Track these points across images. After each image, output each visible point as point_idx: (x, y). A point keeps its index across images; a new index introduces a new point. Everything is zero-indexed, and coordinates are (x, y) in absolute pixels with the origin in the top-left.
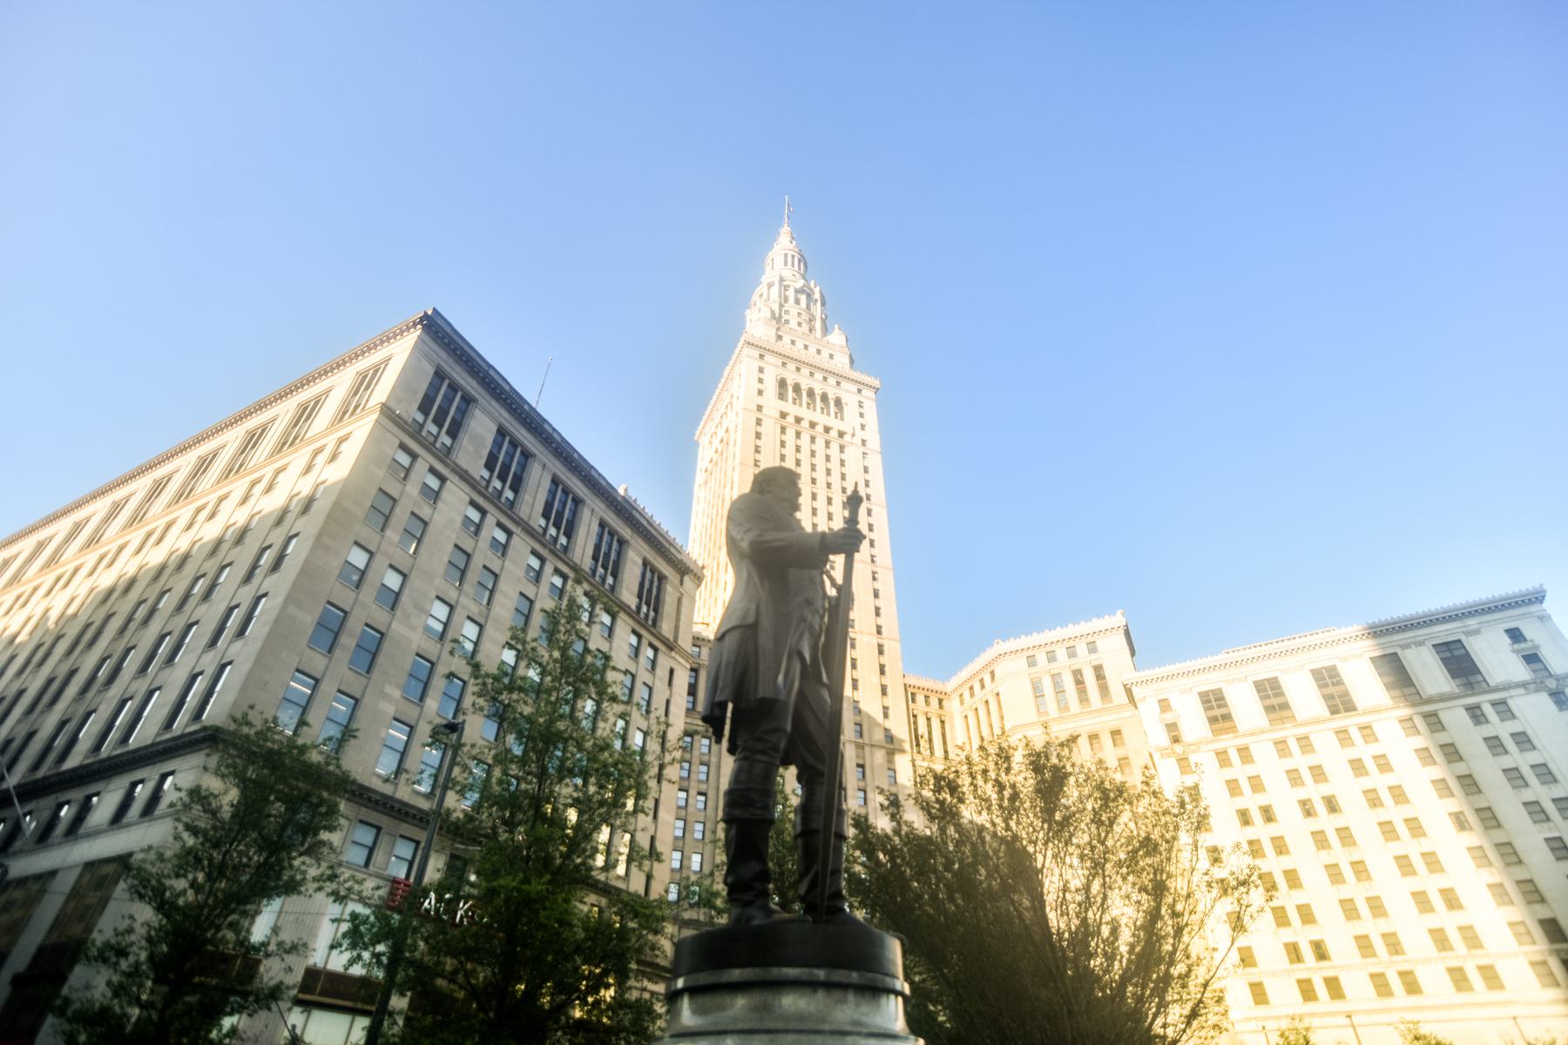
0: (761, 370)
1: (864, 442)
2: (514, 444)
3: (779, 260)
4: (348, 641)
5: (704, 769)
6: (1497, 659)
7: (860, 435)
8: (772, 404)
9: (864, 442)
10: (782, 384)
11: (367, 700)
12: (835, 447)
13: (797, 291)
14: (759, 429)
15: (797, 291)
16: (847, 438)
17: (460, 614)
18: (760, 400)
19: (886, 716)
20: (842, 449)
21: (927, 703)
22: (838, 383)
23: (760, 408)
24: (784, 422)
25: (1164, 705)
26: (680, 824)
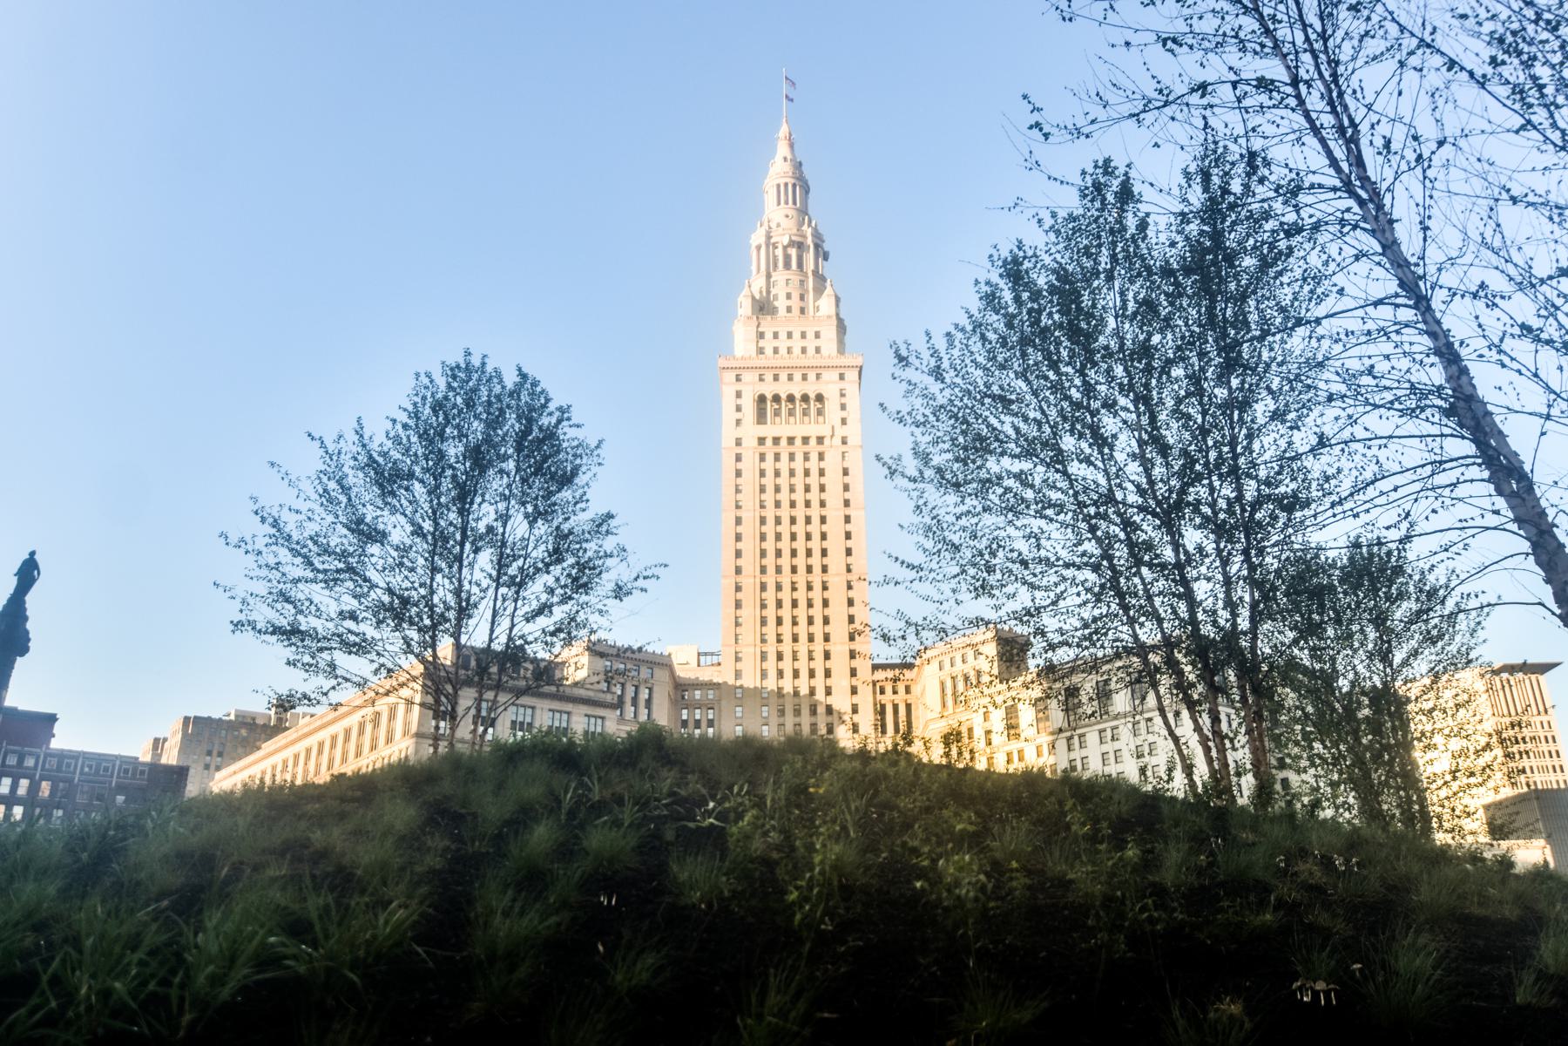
0: (739, 395)
1: (844, 442)
3: (770, 197)
7: (841, 431)
8: (750, 431)
9: (844, 442)
10: (762, 399)
12: (814, 457)
13: (785, 248)
14: (740, 465)
15: (785, 248)
16: (827, 441)
18: (739, 433)
19: (855, 710)
20: (821, 457)
21: (895, 692)
22: (818, 376)
23: (738, 442)
24: (762, 449)
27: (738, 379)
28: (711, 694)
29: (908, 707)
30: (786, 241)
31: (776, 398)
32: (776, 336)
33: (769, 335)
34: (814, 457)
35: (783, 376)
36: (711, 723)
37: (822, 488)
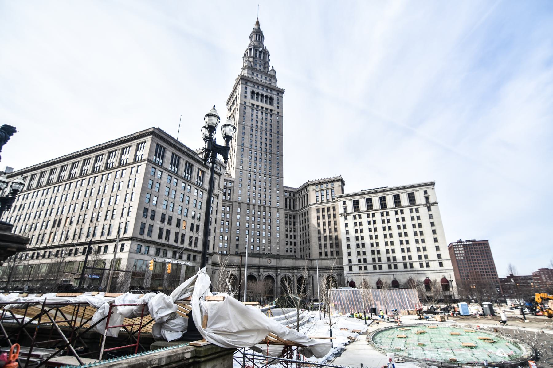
0: (246, 88)
2: (176, 156)
4: (149, 215)
5: (228, 215)
6: (420, 198)
8: (250, 101)
9: (278, 112)
10: (253, 92)
11: (154, 226)
16: (273, 112)
17: (169, 202)
20: (271, 115)
23: (245, 102)
25: (344, 203)
26: (222, 229)
27: (246, 83)
29: (294, 200)
30: (261, 49)
31: (258, 94)
32: (257, 75)
33: (255, 75)
34: (269, 115)
35: (260, 88)
37: (271, 125)
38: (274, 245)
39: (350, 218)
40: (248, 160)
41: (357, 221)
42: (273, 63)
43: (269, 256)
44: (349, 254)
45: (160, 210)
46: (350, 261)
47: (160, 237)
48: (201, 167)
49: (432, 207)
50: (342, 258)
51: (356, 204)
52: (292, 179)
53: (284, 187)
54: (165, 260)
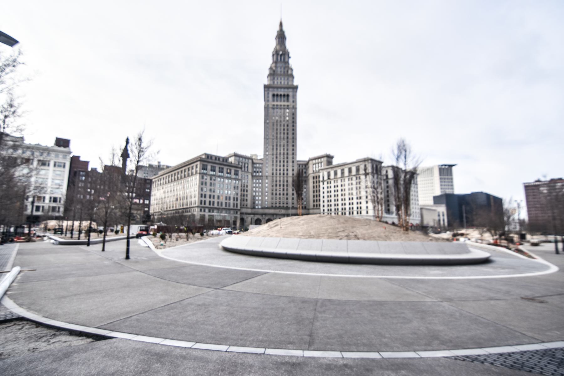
27: (268, 90)
28: (261, 165)
36: (261, 172)
38: (290, 201)
39: (325, 183)
40: (272, 147)
41: (329, 185)
42: (292, 62)
43: (280, 208)
44: (324, 206)
45: (208, 193)
46: (324, 210)
47: (210, 204)
48: (228, 167)
49: (368, 176)
50: (319, 209)
51: (329, 175)
52: (302, 155)
53: (298, 161)
54: (213, 214)
